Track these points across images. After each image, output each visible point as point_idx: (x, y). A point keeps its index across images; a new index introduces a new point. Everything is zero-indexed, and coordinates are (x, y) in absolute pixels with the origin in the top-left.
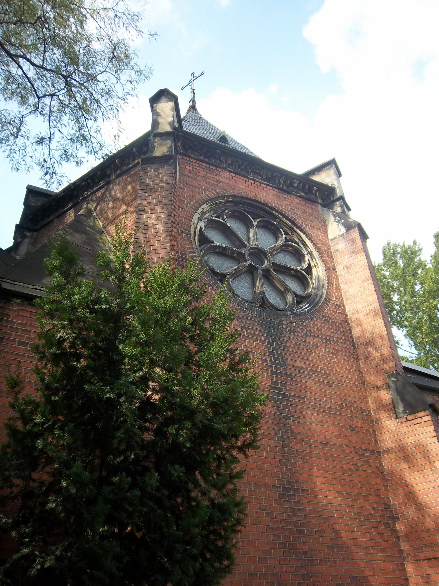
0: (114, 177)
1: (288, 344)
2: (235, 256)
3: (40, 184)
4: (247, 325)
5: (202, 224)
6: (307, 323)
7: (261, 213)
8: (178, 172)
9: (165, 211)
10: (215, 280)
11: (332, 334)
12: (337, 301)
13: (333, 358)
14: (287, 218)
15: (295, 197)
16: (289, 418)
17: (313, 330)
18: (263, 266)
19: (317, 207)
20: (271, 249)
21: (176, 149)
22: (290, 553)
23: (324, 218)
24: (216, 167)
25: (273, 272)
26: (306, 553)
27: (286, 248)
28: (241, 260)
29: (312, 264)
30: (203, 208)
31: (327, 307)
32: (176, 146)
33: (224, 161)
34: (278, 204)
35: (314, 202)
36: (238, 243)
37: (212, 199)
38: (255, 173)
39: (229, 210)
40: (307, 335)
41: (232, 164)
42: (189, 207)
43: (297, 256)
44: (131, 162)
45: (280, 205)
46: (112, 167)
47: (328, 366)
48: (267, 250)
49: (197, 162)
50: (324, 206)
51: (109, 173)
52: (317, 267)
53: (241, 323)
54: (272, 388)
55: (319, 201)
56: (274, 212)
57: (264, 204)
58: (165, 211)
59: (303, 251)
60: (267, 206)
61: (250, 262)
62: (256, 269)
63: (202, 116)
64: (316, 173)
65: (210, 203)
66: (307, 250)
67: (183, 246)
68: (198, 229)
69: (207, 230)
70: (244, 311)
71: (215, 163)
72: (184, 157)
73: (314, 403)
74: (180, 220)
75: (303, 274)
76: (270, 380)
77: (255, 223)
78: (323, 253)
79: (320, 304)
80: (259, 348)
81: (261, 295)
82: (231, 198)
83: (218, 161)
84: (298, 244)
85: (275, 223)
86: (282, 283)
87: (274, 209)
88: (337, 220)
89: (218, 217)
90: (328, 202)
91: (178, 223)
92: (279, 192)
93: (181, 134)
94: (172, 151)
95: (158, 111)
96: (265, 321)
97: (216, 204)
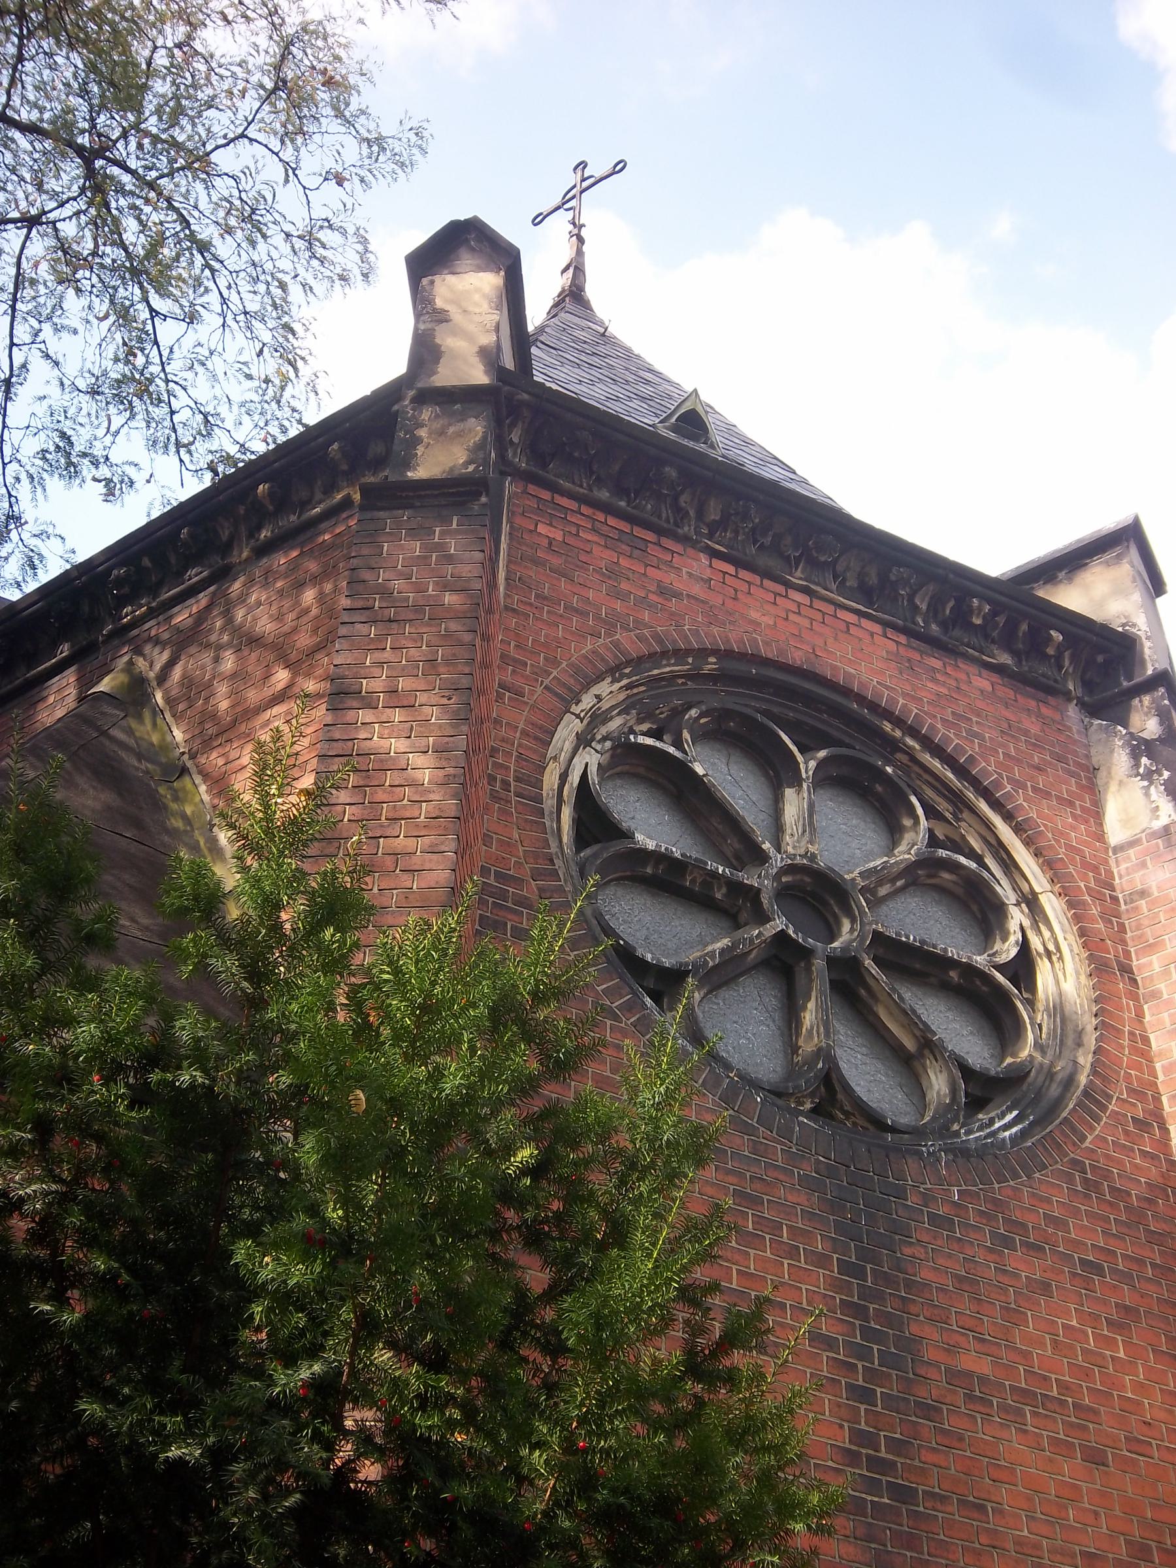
0: (245, 555)
2: (718, 896)
4: (758, 1185)
5: (590, 759)
6: (1010, 1192)
8: (503, 546)
9: (445, 701)
10: (634, 993)
11: (1112, 1241)
12: (1134, 1105)
13: (1111, 1343)
14: (938, 751)
15: (973, 669)
17: (1030, 1220)
18: (835, 945)
20: (868, 878)
21: (502, 456)
24: (660, 532)
25: (874, 970)
27: (930, 876)
28: (744, 916)
29: (1035, 943)
30: (597, 696)
31: (1092, 1128)
32: (501, 443)
33: (692, 513)
34: (905, 695)
36: (733, 844)
37: (638, 662)
38: (813, 563)
39: (704, 708)
40: (1008, 1243)
42: (539, 690)
43: (975, 908)
44: (318, 495)
46: (242, 512)
47: (1087, 1375)
48: (853, 879)
49: (585, 509)
50: (1093, 710)
51: (225, 535)
52: (1054, 958)
53: (731, 1179)
54: (852, 1458)
55: (1071, 687)
56: (887, 727)
57: (846, 692)
58: (445, 701)
59: (998, 888)
60: (861, 699)
61: (779, 923)
62: (806, 954)
63: (613, 330)
64: (1061, 575)
65: (628, 676)
66: (1016, 888)
67: (506, 845)
68: (575, 778)
69: (610, 785)
70: (747, 1129)
71: (654, 519)
72: (532, 488)
73: (1026, 1533)
74: (503, 740)
75: (998, 987)
76: (846, 1425)
77: (808, 766)
78: (1084, 903)
79: (1064, 1114)
80: (804, 1287)
81: (820, 1065)
82: (712, 659)
84: (979, 860)
85: (889, 770)
86: (910, 1019)
87: (888, 715)
88: (1141, 770)
89: (657, 734)
90: (1109, 693)
91: (494, 751)
92: (908, 646)
93: (526, 396)
94: (486, 462)
95: (439, 303)
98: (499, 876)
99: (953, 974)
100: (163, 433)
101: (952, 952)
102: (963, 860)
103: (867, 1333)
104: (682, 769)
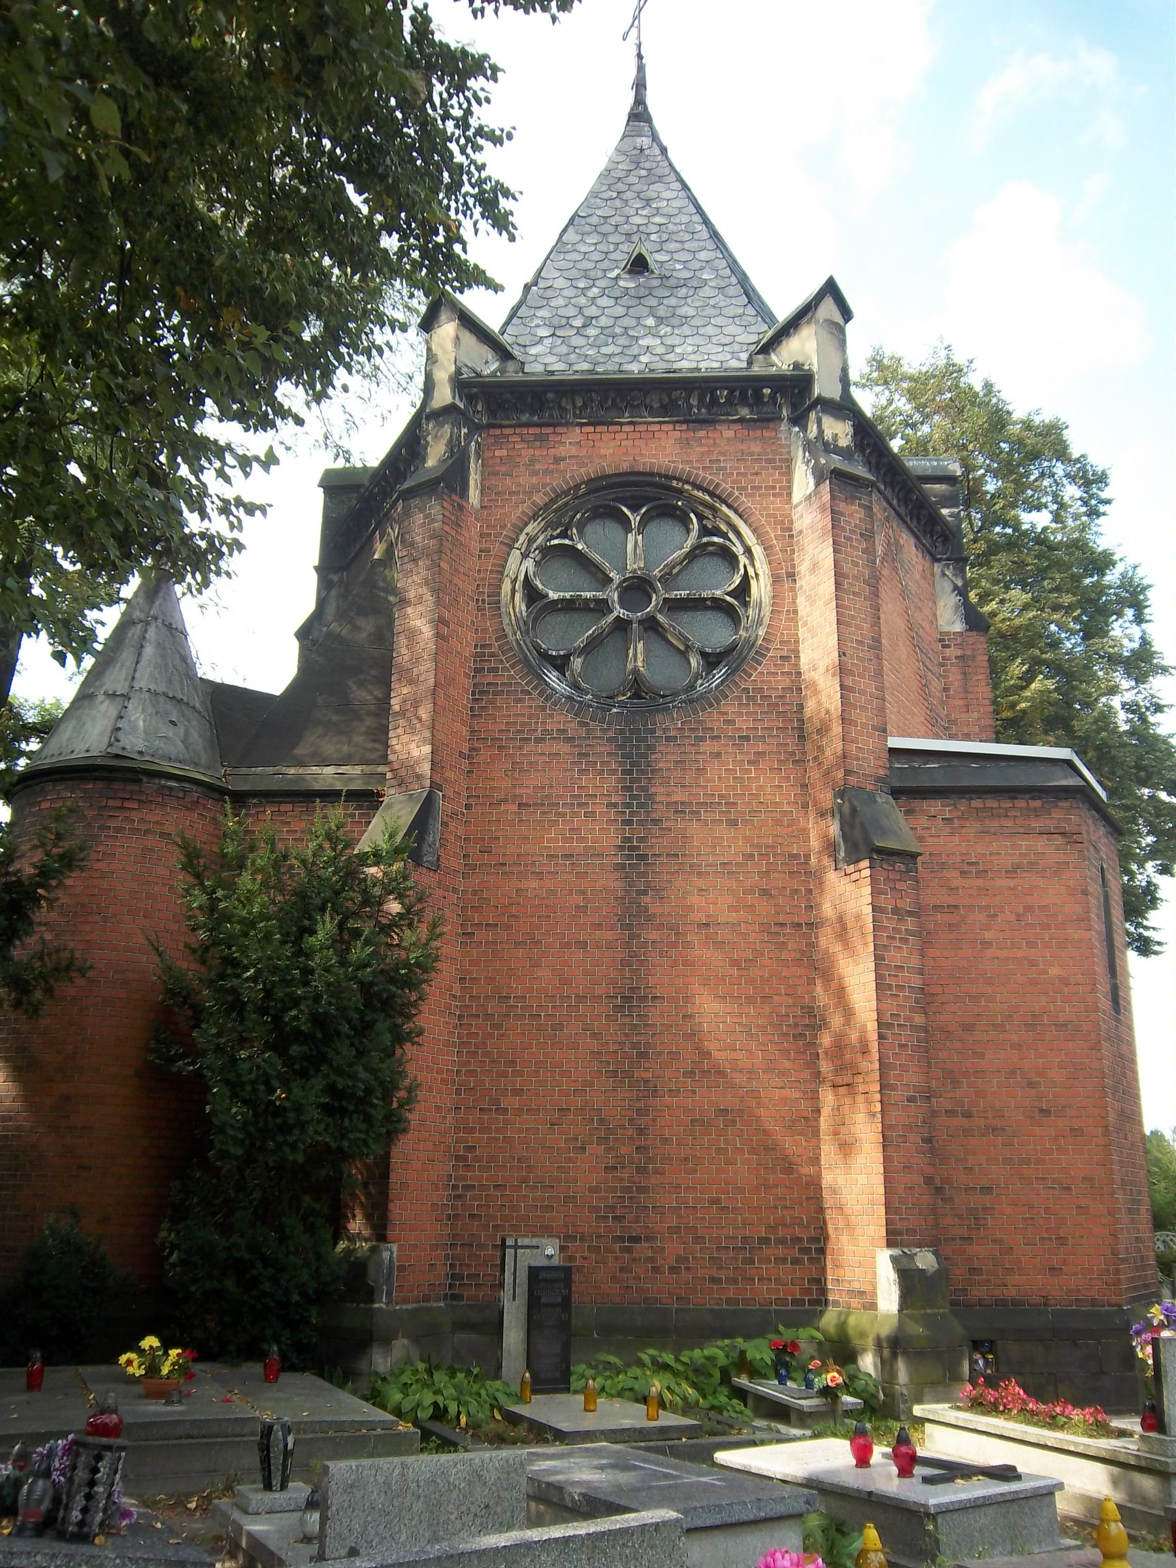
1: (660, 765)
3: (340, 464)
5: (529, 564)
14: (699, 488)
15: (725, 426)
16: (645, 893)
23: (789, 453)
24: (555, 425)
26: (646, 1082)
29: (751, 572)
35: (769, 420)
36: (600, 575)
37: (546, 506)
38: (633, 406)
40: (703, 739)
41: (585, 406)
45: (688, 462)
54: (621, 848)
56: (674, 483)
57: (652, 474)
59: (734, 549)
60: (660, 475)
61: (615, 614)
62: (630, 622)
67: (485, 631)
68: (521, 577)
72: (492, 432)
83: (556, 413)
84: (724, 536)
89: (563, 535)
92: (688, 430)
93: (475, 390)
96: (622, 732)
97: (556, 511)
98: (483, 646)
100: (395, 386)
101: (704, 594)
102: (716, 539)
103: (632, 797)
104: (573, 549)
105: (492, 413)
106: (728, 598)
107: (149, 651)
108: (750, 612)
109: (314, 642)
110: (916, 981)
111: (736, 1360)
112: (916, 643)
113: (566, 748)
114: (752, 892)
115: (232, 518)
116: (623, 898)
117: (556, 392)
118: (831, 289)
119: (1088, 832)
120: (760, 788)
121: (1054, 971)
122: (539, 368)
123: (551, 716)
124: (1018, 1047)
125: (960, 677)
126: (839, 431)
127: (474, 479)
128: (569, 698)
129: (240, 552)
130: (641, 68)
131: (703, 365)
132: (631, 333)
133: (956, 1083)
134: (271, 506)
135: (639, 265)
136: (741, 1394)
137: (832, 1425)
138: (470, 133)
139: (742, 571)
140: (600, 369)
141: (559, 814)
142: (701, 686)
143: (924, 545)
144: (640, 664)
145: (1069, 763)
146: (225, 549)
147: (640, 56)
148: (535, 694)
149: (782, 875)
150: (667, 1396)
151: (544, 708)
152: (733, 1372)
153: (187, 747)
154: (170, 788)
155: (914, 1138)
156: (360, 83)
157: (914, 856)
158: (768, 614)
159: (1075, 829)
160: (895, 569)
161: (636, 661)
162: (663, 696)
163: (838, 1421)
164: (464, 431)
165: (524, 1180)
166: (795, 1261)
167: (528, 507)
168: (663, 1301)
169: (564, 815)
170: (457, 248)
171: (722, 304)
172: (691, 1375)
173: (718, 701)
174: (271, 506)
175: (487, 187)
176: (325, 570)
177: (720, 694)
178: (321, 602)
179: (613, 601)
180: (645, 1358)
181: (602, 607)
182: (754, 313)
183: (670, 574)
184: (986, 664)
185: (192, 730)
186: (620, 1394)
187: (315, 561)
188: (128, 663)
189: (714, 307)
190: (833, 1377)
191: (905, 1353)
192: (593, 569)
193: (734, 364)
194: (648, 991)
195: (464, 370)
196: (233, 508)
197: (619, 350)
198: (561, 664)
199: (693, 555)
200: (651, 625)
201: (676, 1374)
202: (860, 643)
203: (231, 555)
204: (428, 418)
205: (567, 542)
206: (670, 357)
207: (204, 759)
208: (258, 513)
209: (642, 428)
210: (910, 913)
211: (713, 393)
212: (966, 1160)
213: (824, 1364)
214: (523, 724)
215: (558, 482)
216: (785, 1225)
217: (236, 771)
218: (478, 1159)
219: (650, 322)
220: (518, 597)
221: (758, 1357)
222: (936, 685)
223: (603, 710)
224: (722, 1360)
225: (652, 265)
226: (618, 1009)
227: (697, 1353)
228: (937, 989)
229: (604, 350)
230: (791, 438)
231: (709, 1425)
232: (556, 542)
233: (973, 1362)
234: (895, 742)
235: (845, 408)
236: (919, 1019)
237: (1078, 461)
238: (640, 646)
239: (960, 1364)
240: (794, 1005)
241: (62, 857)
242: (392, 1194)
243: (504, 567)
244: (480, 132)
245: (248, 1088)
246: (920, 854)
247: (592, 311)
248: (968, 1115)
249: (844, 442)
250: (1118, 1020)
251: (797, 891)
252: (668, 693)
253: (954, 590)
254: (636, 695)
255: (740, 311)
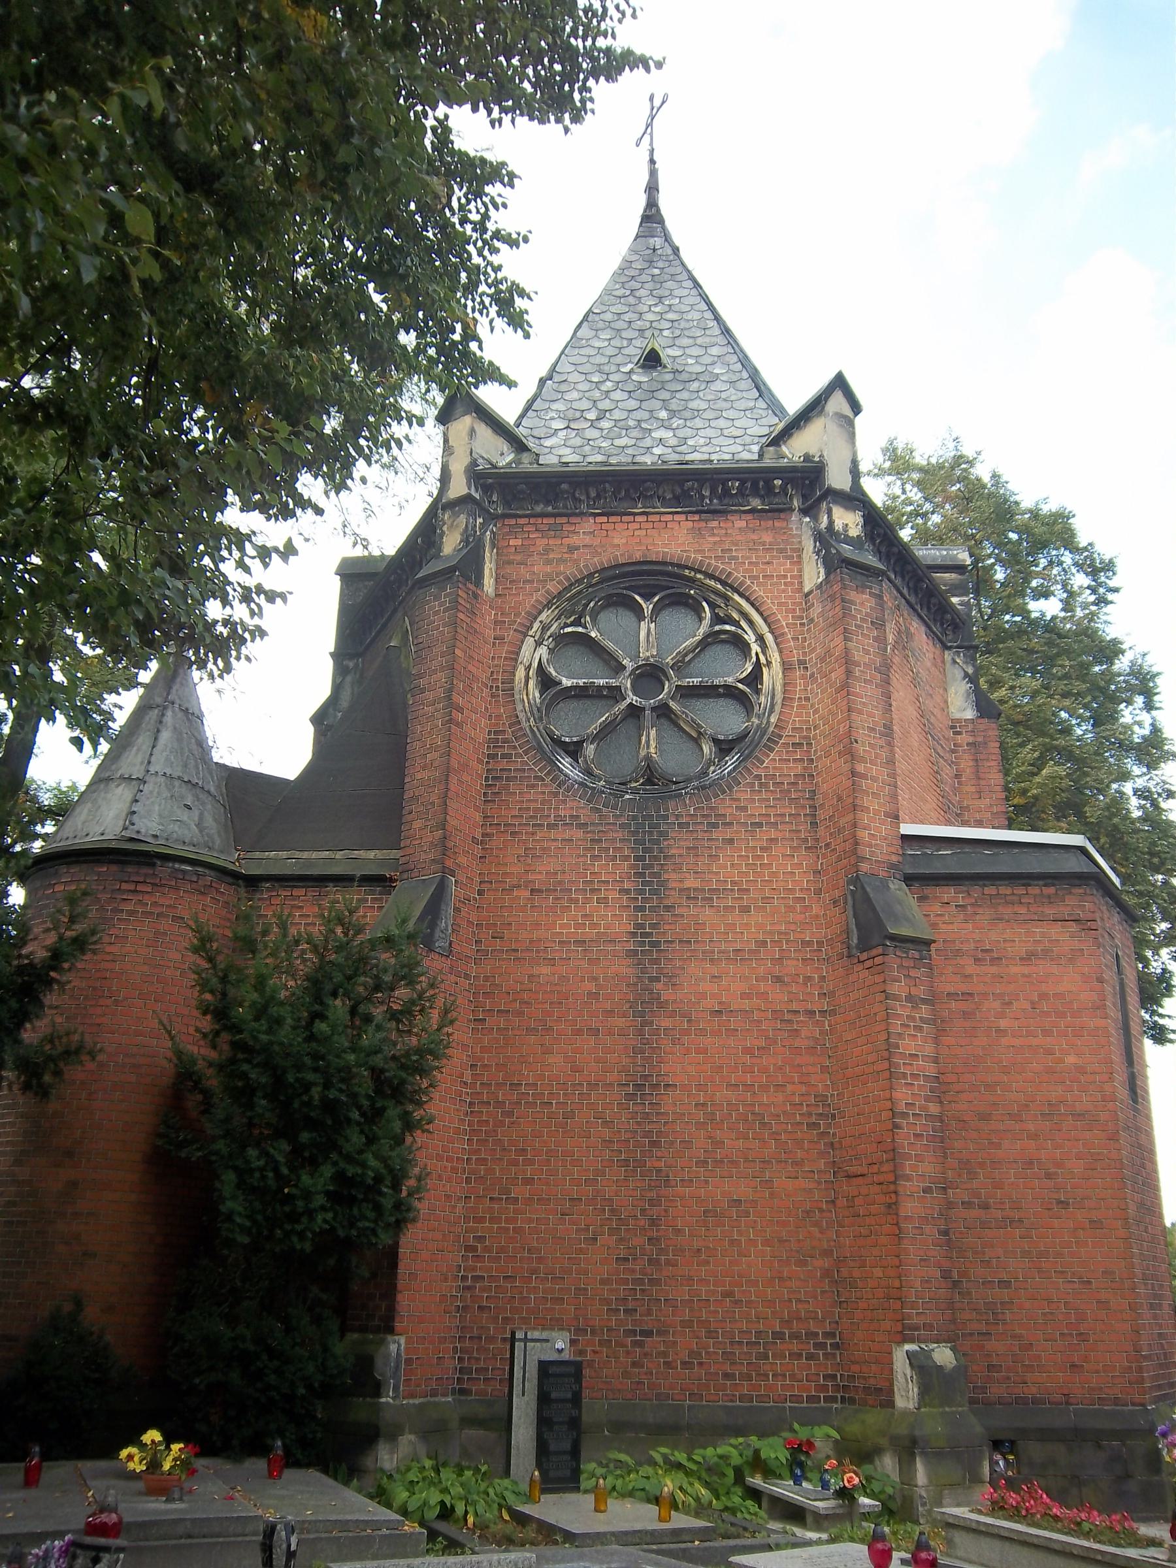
1: (673, 852)
3: (359, 552)
5: (543, 651)
7: (663, 580)
14: (712, 577)
15: (736, 517)
16: (658, 979)
17: (728, 812)
19: (787, 520)
22: (635, 1171)
23: (800, 542)
26: (659, 1171)
29: (763, 659)
36: (613, 663)
38: (646, 497)
40: (715, 825)
41: (598, 496)
45: (699, 551)
50: (805, 512)
54: (634, 934)
56: (687, 572)
57: (665, 563)
59: (746, 637)
60: (672, 564)
61: (628, 701)
62: (643, 709)
67: (499, 717)
68: (535, 664)
83: (570, 504)
84: (736, 624)
96: (634, 818)
97: (569, 599)
99: (721, 690)
101: (716, 682)
102: (727, 627)
104: (586, 637)
105: (507, 504)
106: (740, 686)
107: (165, 736)
108: (763, 699)
109: (329, 728)
110: (931, 1070)
111: (750, 1459)
112: (927, 731)
113: (580, 834)
114: (765, 979)
115: (253, 605)
116: (635, 985)
117: (570, 483)
118: (839, 383)
119: (1102, 919)
120: (774, 874)
121: (1071, 1059)
122: (554, 460)
123: (564, 802)
124: (1034, 1136)
125: (971, 763)
126: (848, 521)
127: (489, 568)
128: (581, 784)
129: (262, 639)
130: (653, 173)
131: (714, 457)
132: (644, 425)
133: (973, 1175)
134: (291, 593)
135: (652, 360)
136: (755, 1494)
137: (849, 1529)
138: (487, 236)
139: (754, 659)
140: (613, 460)
141: (571, 900)
142: (714, 773)
143: (934, 633)
144: (652, 750)
145: (1082, 850)
146: (247, 635)
147: (652, 162)
148: (548, 780)
149: (795, 963)
150: (680, 1496)
151: (556, 794)
152: (746, 1472)
153: (201, 831)
154: (184, 872)
155: (931, 1231)
156: (384, 189)
157: (927, 943)
158: (780, 701)
159: (1090, 916)
160: (906, 657)
161: (648, 747)
162: (676, 783)
163: (856, 1524)
164: (479, 520)
165: (534, 1271)
166: (810, 1357)
167: (542, 595)
168: (676, 1397)
169: (576, 901)
170: (473, 346)
171: (733, 398)
172: (704, 1475)
173: (730, 788)
174: (291, 593)
175: (503, 287)
176: (338, 656)
177: (733, 780)
178: (337, 688)
179: (626, 688)
180: (659, 1459)
181: (615, 694)
182: (765, 406)
183: (683, 661)
184: (997, 751)
185: (206, 813)
186: (631, 1494)
187: (331, 646)
188: (144, 747)
189: (725, 400)
190: (851, 1479)
191: (924, 1454)
192: (606, 657)
193: (746, 456)
194: (660, 1079)
195: (480, 461)
196: (254, 595)
197: (633, 442)
198: (574, 751)
199: (706, 643)
200: (663, 711)
201: (688, 1473)
202: (872, 730)
203: (253, 641)
204: (444, 508)
205: (580, 629)
206: (683, 449)
207: (218, 842)
208: (278, 600)
209: (656, 518)
210: (924, 1001)
211: (724, 483)
212: (984, 1253)
213: (840, 1463)
214: (536, 810)
215: (571, 571)
216: (799, 1319)
217: (249, 855)
218: (487, 1249)
219: (663, 414)
220: (531, 683)
221: (773, 1456)
222: (947, 772)
223: (616, 796)
224: (736, 1460)
225: (664, 360)
226: (630, 1097)
227: (710, 1451)
228: (951, 1078)
229: (617, 442)
230: (801, 530)
231: (723, 1527)
232: (569, 629)
233: (993, 1463)
234: (907, 829)
235: (856, 499)
236: (934, 1109)
237: (1085, 549)
238: (653, 732)
239: (980, 1465)
240: (809, 1094)
241: (75, 940)
242: (400, 1284)
243: (518, 654)
244: (497, 235)
245: (257, 1175)
246: (934, 942)
247: (605, 404)
248: (985, 1206)
249: (854, 532)
250: (1136, 1110)
251: (809, 979)
252: (680, 779)
253: (964, 678)
254: (649, 781)
255: (751, 404)
